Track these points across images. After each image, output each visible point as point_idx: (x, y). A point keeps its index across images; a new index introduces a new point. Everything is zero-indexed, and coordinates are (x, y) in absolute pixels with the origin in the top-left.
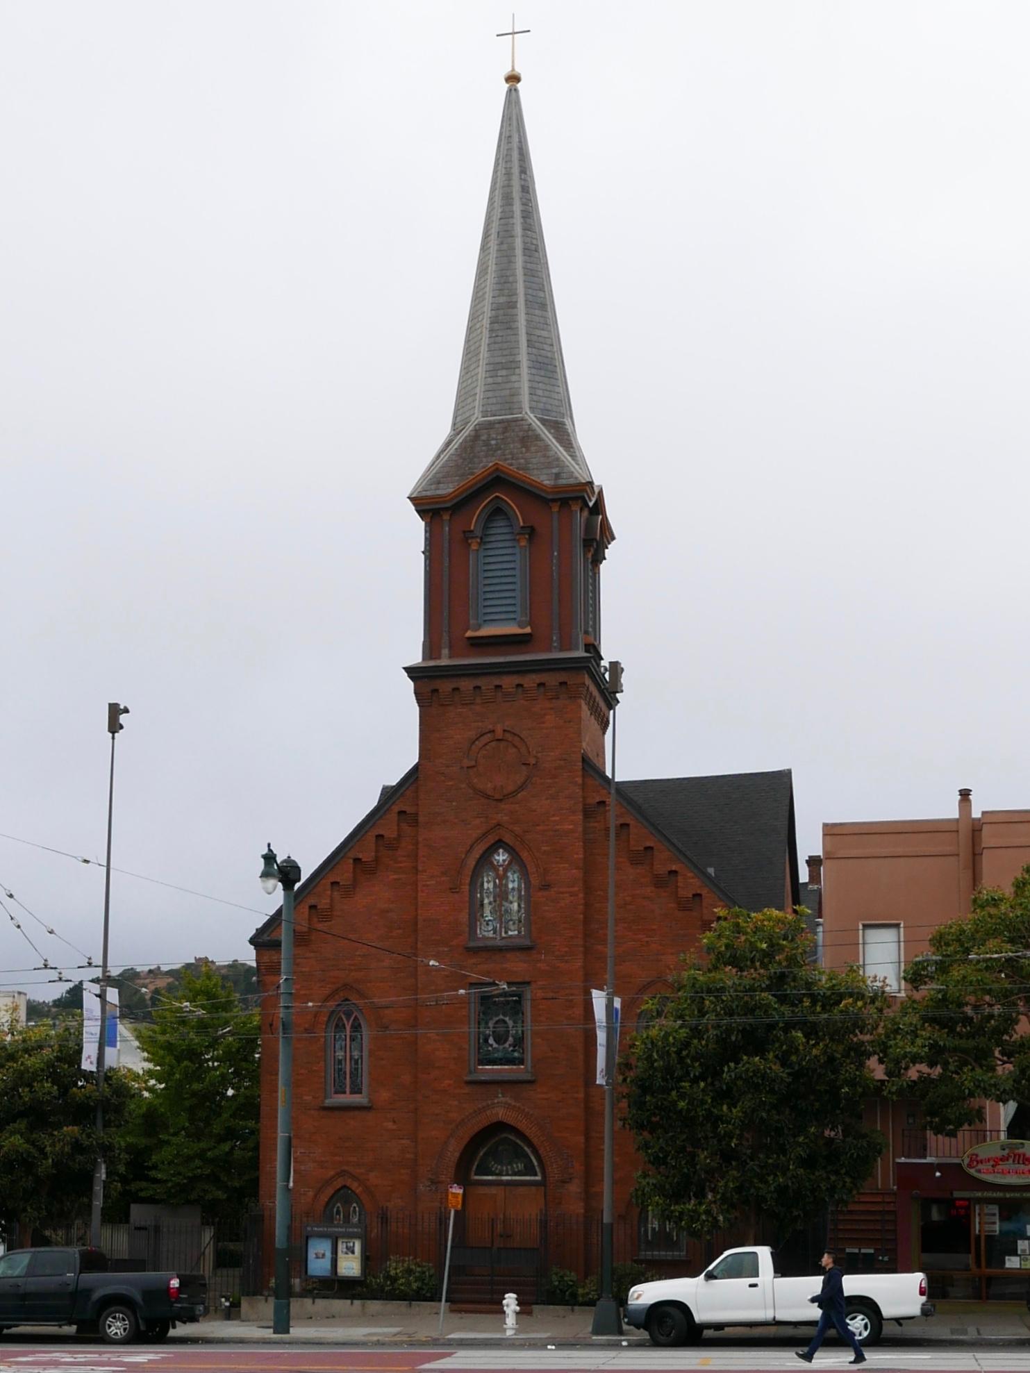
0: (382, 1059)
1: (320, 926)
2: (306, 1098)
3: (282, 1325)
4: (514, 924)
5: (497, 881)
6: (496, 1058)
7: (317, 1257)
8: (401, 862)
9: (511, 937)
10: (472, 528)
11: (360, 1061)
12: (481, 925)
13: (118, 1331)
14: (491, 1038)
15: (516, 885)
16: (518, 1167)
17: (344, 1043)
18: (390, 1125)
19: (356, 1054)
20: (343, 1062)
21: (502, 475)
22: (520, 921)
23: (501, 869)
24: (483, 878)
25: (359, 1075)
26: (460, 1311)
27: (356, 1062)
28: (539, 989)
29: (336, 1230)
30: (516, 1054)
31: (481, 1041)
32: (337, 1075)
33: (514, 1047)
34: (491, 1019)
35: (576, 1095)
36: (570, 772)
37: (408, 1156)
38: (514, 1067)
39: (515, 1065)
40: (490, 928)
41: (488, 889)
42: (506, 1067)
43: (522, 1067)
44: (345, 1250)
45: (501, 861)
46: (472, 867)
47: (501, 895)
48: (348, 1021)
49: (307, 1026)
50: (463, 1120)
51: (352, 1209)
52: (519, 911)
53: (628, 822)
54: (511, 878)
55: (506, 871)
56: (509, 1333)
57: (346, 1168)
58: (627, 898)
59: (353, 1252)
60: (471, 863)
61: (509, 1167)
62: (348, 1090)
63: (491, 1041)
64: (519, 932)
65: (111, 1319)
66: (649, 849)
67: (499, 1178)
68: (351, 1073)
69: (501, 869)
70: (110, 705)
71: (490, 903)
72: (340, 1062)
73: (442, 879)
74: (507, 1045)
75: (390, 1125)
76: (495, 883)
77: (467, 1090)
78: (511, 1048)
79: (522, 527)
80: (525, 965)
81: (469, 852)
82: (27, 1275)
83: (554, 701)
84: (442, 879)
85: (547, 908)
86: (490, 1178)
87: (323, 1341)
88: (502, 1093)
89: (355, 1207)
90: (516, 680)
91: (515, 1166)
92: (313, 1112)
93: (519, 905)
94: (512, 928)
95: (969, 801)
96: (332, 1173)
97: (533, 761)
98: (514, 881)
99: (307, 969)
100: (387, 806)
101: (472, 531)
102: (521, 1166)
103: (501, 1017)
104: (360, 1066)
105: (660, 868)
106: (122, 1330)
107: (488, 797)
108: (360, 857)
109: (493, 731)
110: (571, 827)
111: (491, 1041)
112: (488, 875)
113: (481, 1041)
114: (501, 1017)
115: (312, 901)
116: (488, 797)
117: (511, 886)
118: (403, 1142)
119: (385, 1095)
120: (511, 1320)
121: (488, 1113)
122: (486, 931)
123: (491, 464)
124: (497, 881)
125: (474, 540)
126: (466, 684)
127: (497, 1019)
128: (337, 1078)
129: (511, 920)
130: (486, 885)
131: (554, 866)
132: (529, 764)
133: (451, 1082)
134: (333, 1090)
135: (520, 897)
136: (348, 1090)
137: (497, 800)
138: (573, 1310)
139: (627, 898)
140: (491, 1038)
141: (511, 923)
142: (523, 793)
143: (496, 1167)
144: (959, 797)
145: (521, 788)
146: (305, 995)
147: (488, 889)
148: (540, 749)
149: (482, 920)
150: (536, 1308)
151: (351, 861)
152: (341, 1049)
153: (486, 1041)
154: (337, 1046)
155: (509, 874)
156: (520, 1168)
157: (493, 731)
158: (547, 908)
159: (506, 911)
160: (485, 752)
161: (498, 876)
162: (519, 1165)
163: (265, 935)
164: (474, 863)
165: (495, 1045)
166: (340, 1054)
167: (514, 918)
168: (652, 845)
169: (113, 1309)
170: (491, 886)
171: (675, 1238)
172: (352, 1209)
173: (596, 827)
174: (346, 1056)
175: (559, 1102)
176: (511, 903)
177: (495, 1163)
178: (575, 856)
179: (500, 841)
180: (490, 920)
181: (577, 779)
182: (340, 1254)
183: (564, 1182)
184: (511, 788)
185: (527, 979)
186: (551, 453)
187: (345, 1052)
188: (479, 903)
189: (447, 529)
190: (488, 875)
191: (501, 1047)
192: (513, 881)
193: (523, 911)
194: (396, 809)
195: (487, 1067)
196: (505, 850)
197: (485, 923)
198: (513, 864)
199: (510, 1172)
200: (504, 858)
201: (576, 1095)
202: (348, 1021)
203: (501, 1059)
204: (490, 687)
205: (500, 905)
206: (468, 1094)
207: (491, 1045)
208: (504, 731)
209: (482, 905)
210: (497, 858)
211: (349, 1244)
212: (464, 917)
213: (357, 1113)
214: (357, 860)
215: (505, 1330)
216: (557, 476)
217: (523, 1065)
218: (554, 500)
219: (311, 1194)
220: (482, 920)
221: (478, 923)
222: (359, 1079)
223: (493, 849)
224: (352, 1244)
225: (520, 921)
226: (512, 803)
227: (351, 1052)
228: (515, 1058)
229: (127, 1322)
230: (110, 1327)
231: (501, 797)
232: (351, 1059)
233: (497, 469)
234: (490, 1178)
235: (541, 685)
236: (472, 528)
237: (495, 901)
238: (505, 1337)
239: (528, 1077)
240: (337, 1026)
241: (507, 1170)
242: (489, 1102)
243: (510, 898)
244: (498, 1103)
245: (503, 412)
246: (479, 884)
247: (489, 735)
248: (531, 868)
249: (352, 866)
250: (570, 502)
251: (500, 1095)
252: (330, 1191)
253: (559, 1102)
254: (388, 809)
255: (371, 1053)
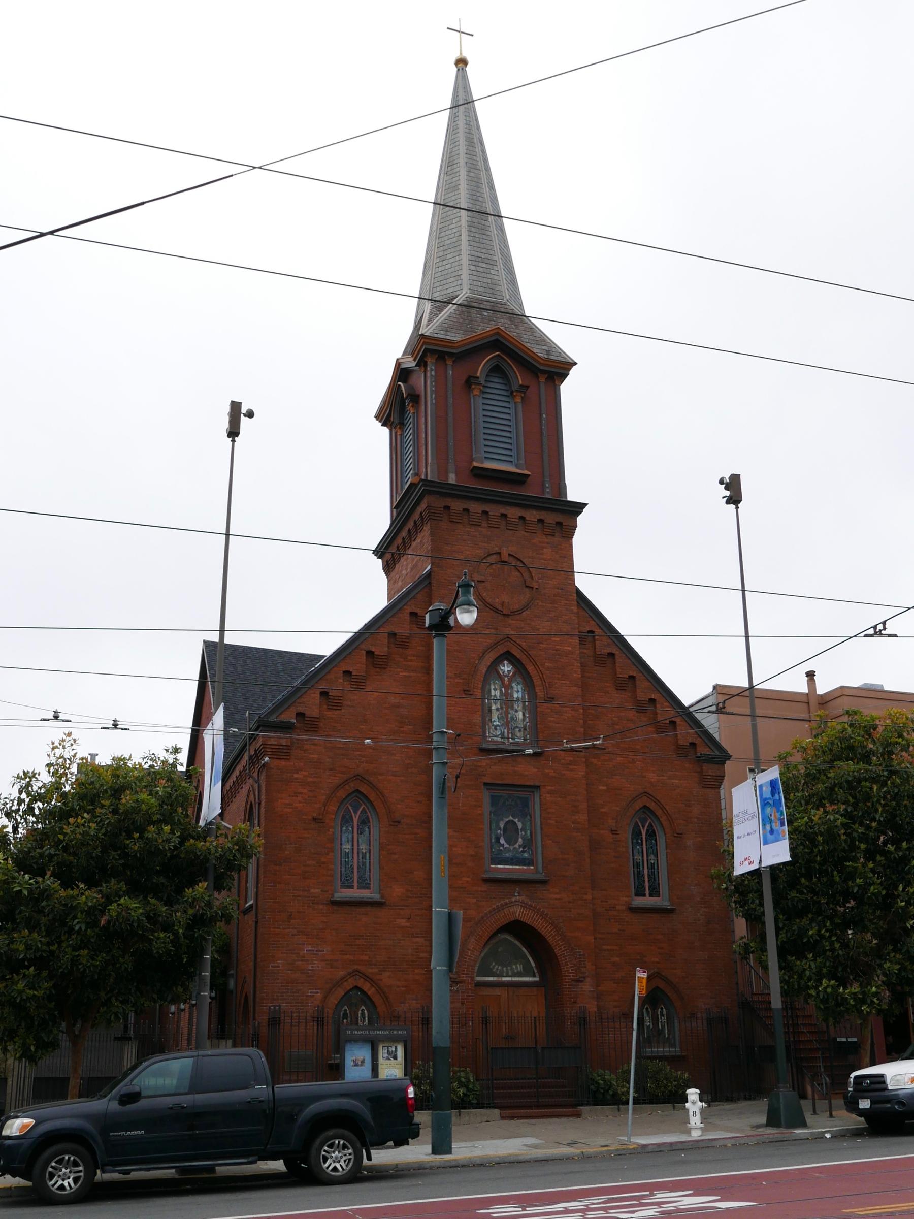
0: (394, 854)
1: (329, 714)
2: (312, 891)
3: (441, 1145)
4: (520, 731)
5: (503, 689)
6: (508, 858)
7: (356, 1065)
8: (411, 661)
9: (517, 743)
10: (478, 375)
11: (368, 855)
12: (489, 729)
13: (338, 1166)
14: (502, 838)
15: (520, 695)
16: (517, 967)
17: (350, 836)
18: (403, 922)
19: (364, 847)
20: (350, 856)
21: (501, 340)
22: (525, 729)
23: (506, 678)
24: (490, 685)
25: (367, 869)
26: (512, 1118)
27: (364, 857)
28: (548, 793)
29: (380, 1032)
30: (526, 855)
31: (493, 840)
32: (343, 869)
33: (523, 848)
34: (502, 820)
35: (585, 897)
36: (567, 600)
37: (422, 955)
38: (525, 867)
39: (524, 865)
40: (498, 733)
41: (495, 696)
42: (517, 867)
43: (532, 867)
44: (386, 1055)
45: (506, 671)
46: (484, 672)
47: (507, 702)
48: (356, 812)
49: (315, 815)
50: (482, 918)
51: (360, 1012)
52: (524, 720)
53: (614, 652)
54: (516, 689)
55: (510, 681)
56: (696, 1134)
57: (359, 967)
58: (614, 719)
59: (395, 1058)
60: (483, 669)
61: (509, 968)
62: (356, 884)
63: (502, 841)
64: (525, 740)
65: (326, 1148)
66: (632, 678)
67: (500, 979)
68: (359, 867)
69: (506, 678)
70: (233, 402)
71: (497, 709)
72: (347, 854)
73: (456, 680)
74: (517, 846)
75: (403, 922)
76: (501, 691)
77: (484, 888)
78: (521, 849)
79: (521, 386)
80: (536, 770)
81: (481, 658)
82: (194, 1089)
83: (550, 537)
84: (456, 680)
85: (552, 719)
86: (491, 979)
87: (521, 1158)
88: (519, 893)
89: (363, 1010)
90: (519, 512)
91: (514, 966)
92: (321, 907)
93: (524, 715)
94: (518, 735)
95: (814, 680)
96: (342, 973)
97: (535, 585)
98: (518, 692)
99: (316, 756)
100: (400, 605)
101: (478, 378)
102: (520, 967)
103: (511, 818)
104: (368, 861)
105: (642, 696)
106: (342, 1163)
107: (496, 611)
108: (373, 650)
109: (499, 553)
110: (570, 648)
111: (502, 841)
112: (495, 683)
113: (493, 840)
114: (511, 818)
115: (323, 686)
116: (496, 611)
117: (515, 696)
118: (418, 940)
119: (398, 890)
120: (695, 1121)
121: (506, 910)
122: (495, 733)
123: (488, 329)
124: (503, 689)
125: (478, 387)
126: (476, 508)
127: (507, 820)
128: (343, 872)
129: (517, 727)
130: (493, 693)
131: (556, 681)
132: (532, 588)
133: (469, 879)
134: (340, 884)
135: (524, 707)
136: (356, 884)
137: (504, 615)
138: (619, 1110)
139: (614, 719)
140: (502, 838)
141: (517, 730)
142: (528, 612)
143: (497, 968)
144: (807, 678)
145: (526, 607)
146: (314, 782)
147: (495, 696)
148: (540, 576)
149: (490, 724)
150: (585, 1109)
151: (364, 653)
152: (348, 842)
153: (498, 840)
154: (343, 839)
155: (514, 685)
156: (519, 969)
157: (499, 553)
158: (552, 719)
159: (512, 718)
160: (491, 571)
161: (503, 685)
162: (518, 965)
163: (275, 716)
164: (486, 670)
165: (506, 845)
166: (347, 847)
167: (520, 726)
168: (635, 674)
169: (331, 1133)
170: (498, 693)
171: (667, 1036)
172: (360, 1012)
173: (586, 653)
174: (353, 849)
175: (569, 902)
176: (517, 711)
177: (496, 964)
178: (575, 675)
179: (508, 653)
180: (498, 725)
181: (572, 608)
182: (381, 1060)
183: (578, 981)
184: (517, 607)
185: (537, 784)
186: (538, 335)
187: (353, 845)
188: (487, 708)
189: (451, 372)
190: (495, 683)
191: (512, 848)
192: (518, 692)
193: (527, 720)
194: (408, 609)
195: (499, 866)
196: (510, 662)
197: (493, 728)
198: (517, 676)
199: (510, 974)
200: (509, 669)
201: (585, 897)
202: (356, 812)
203: (512, 859)
204: (496, 514)
205: (507, 713)
206: (486, 891)
207: (503, 845)
208: (509, 555)
209: (490, 710)
210: (502, 668)
211: (390, 1049)
212: (477, 719)
213: (369, 908)
214: (370, 653)
215: (688, 1131)
216: (548, 352)
217: (533, 865)
218: (544, 372)
219: (319, 996)
220: (490, 724)
221: (487, 727)
222: (367, 873)
223: (498, 661)
224: (393, 1049)
225: (525, 729)
226: (517, 620)
227: (358, 845)
228: (525, 859)
229: (350, 1151)
230: (325, 1159)
231: (510, 613)
232: (358, 853)
233: (498, 333)
234: (491, 979)
235: (541, 521)
236: (478, 375)
237: (502, 708)
238: (690, 1139)
239: (541, 877)
240: (343, 817)
241: (507, 973)
242: (507, 900)
243: (516, 707)
244: (515, 901)
245: (483, 294)
246: (487, 691)
247: (494, 556)
248: (537, 681)
249: (365, 657)
250: (555, 377)
251: (516, 894)
252: (341, 992)
253: (569, 902)
254: (401, 608)
255: (382, 847)
